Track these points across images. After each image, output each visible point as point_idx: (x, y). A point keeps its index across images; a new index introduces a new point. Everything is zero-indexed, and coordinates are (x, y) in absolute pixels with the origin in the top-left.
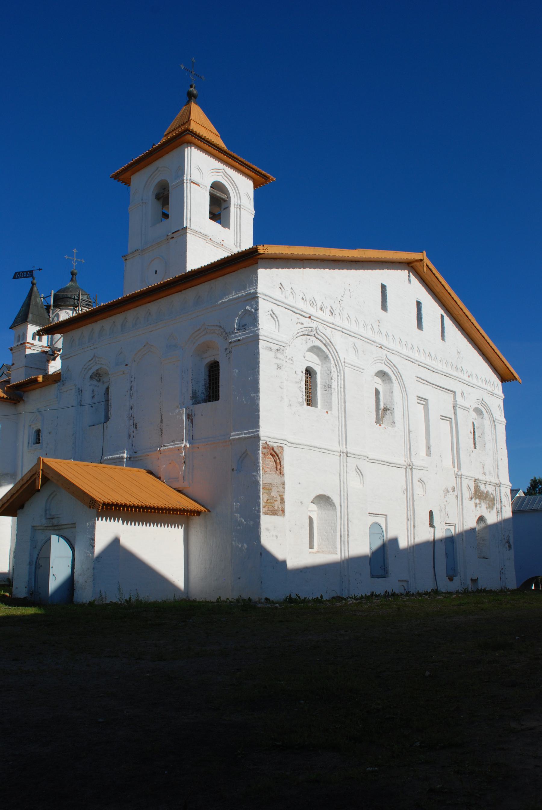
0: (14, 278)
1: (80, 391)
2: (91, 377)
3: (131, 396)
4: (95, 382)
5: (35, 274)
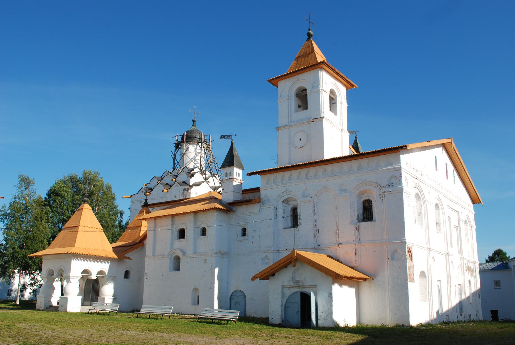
0: (221, 138)
1: (276, 209)
2: (283, 202)
3: (314, 214)
4: (285, 204)
5: (233, 137)
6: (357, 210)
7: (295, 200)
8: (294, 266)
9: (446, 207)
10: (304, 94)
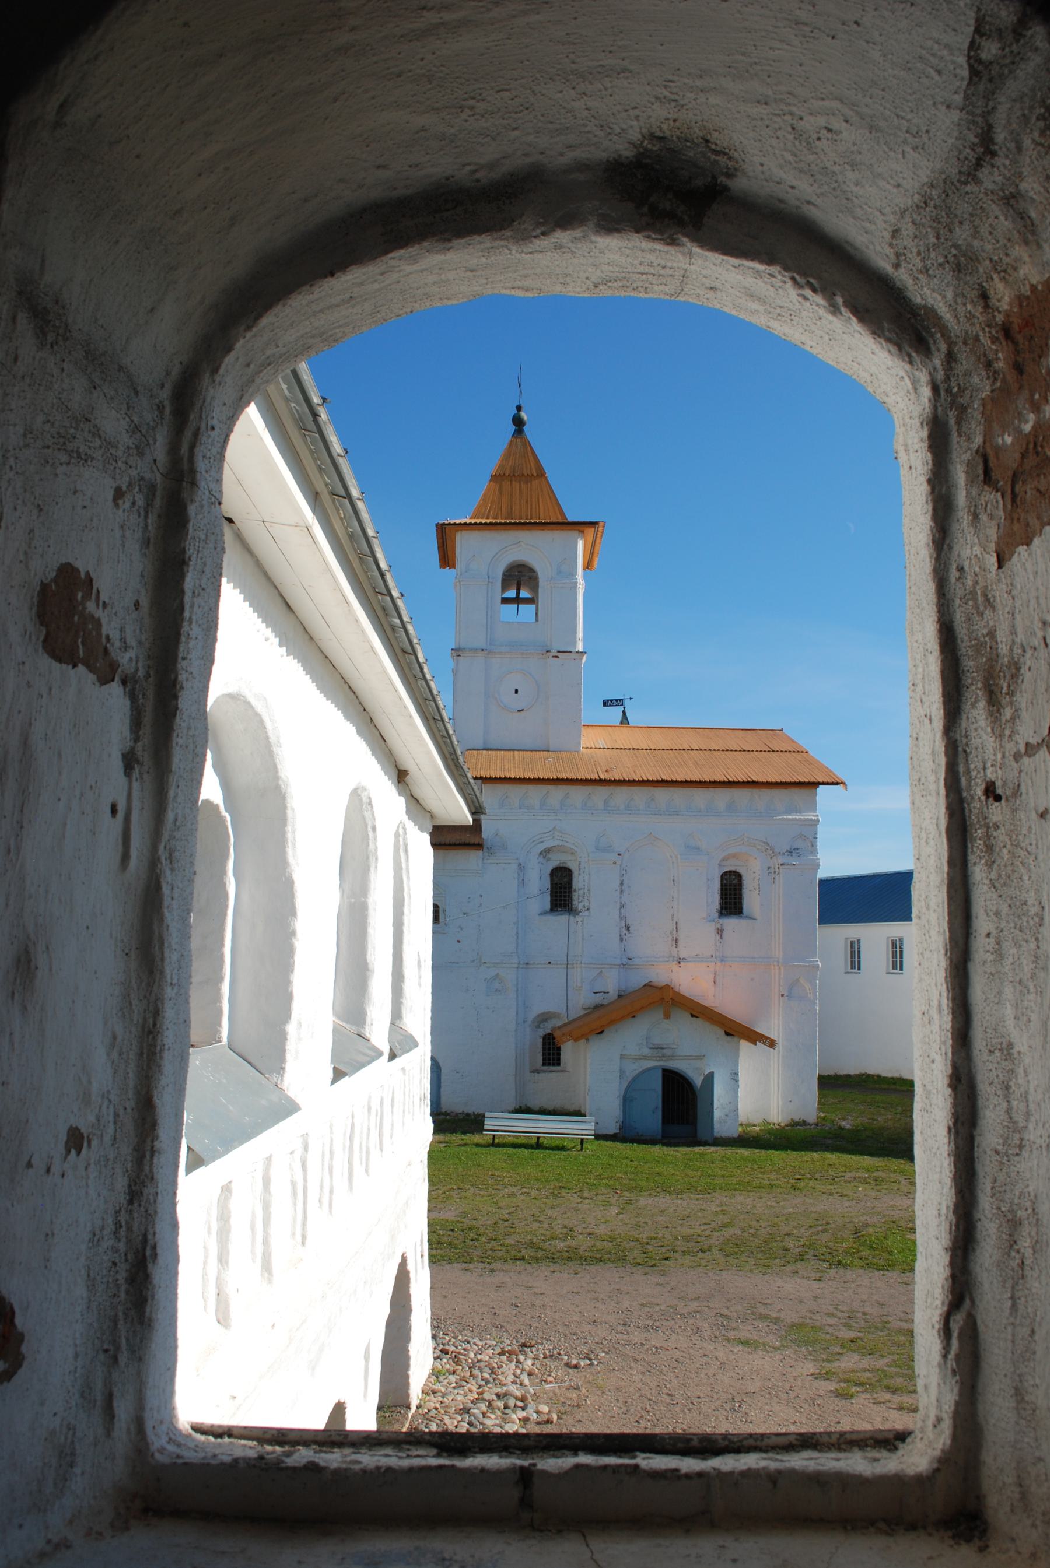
3: (622, 892)
4: (541, 859)
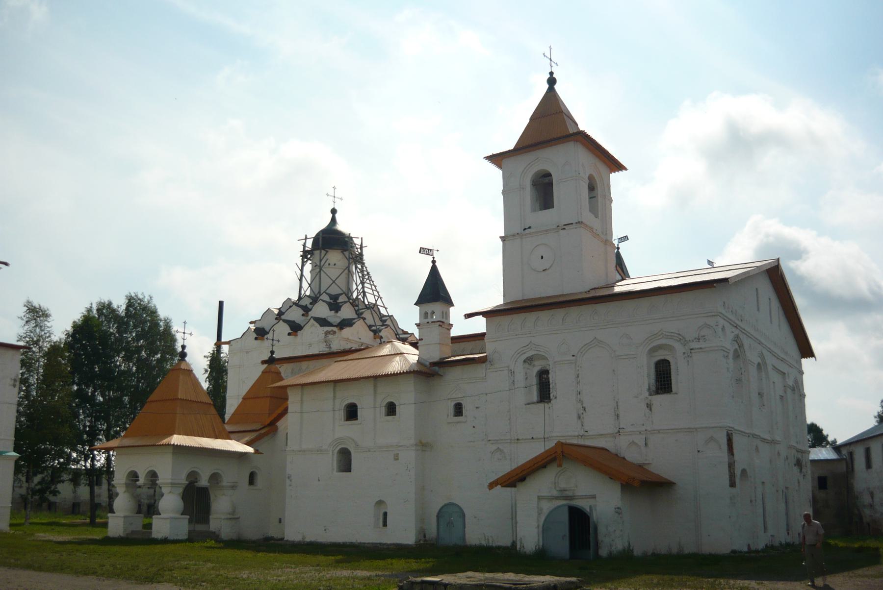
1: (512, 373)
2: (525, 361)
3: (578, 383)
4: (527, 365)
5: (435, 253)
6: (646, 377)
7: (544, 358)
8: (560, 466)
9: (770, 368)
10: (547, 180)
